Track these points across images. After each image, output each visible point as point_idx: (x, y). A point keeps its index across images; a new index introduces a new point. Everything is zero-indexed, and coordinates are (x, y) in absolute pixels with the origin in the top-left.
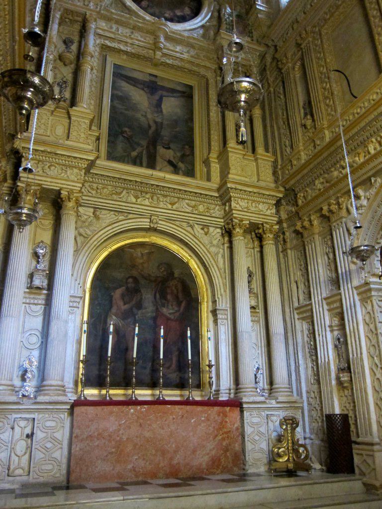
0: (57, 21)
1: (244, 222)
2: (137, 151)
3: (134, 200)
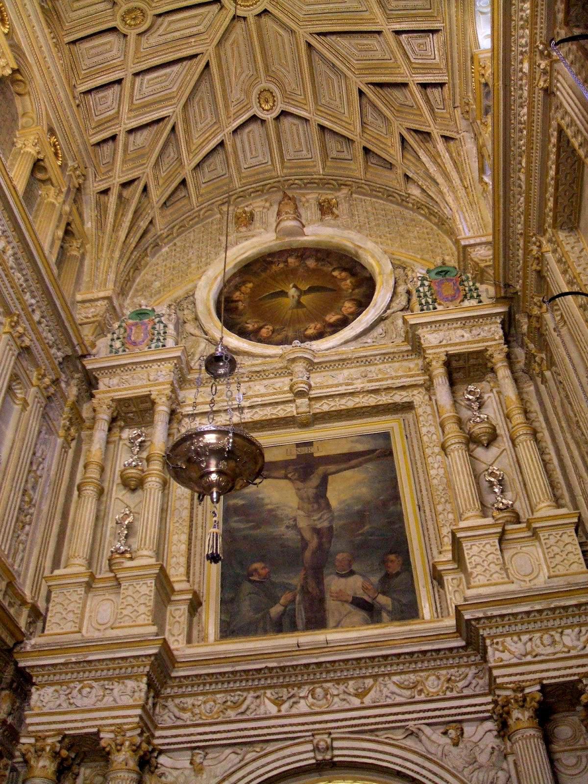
0: (105, 426)
1: (527, 691)
2: (282, 601)
3: (273, 709)
